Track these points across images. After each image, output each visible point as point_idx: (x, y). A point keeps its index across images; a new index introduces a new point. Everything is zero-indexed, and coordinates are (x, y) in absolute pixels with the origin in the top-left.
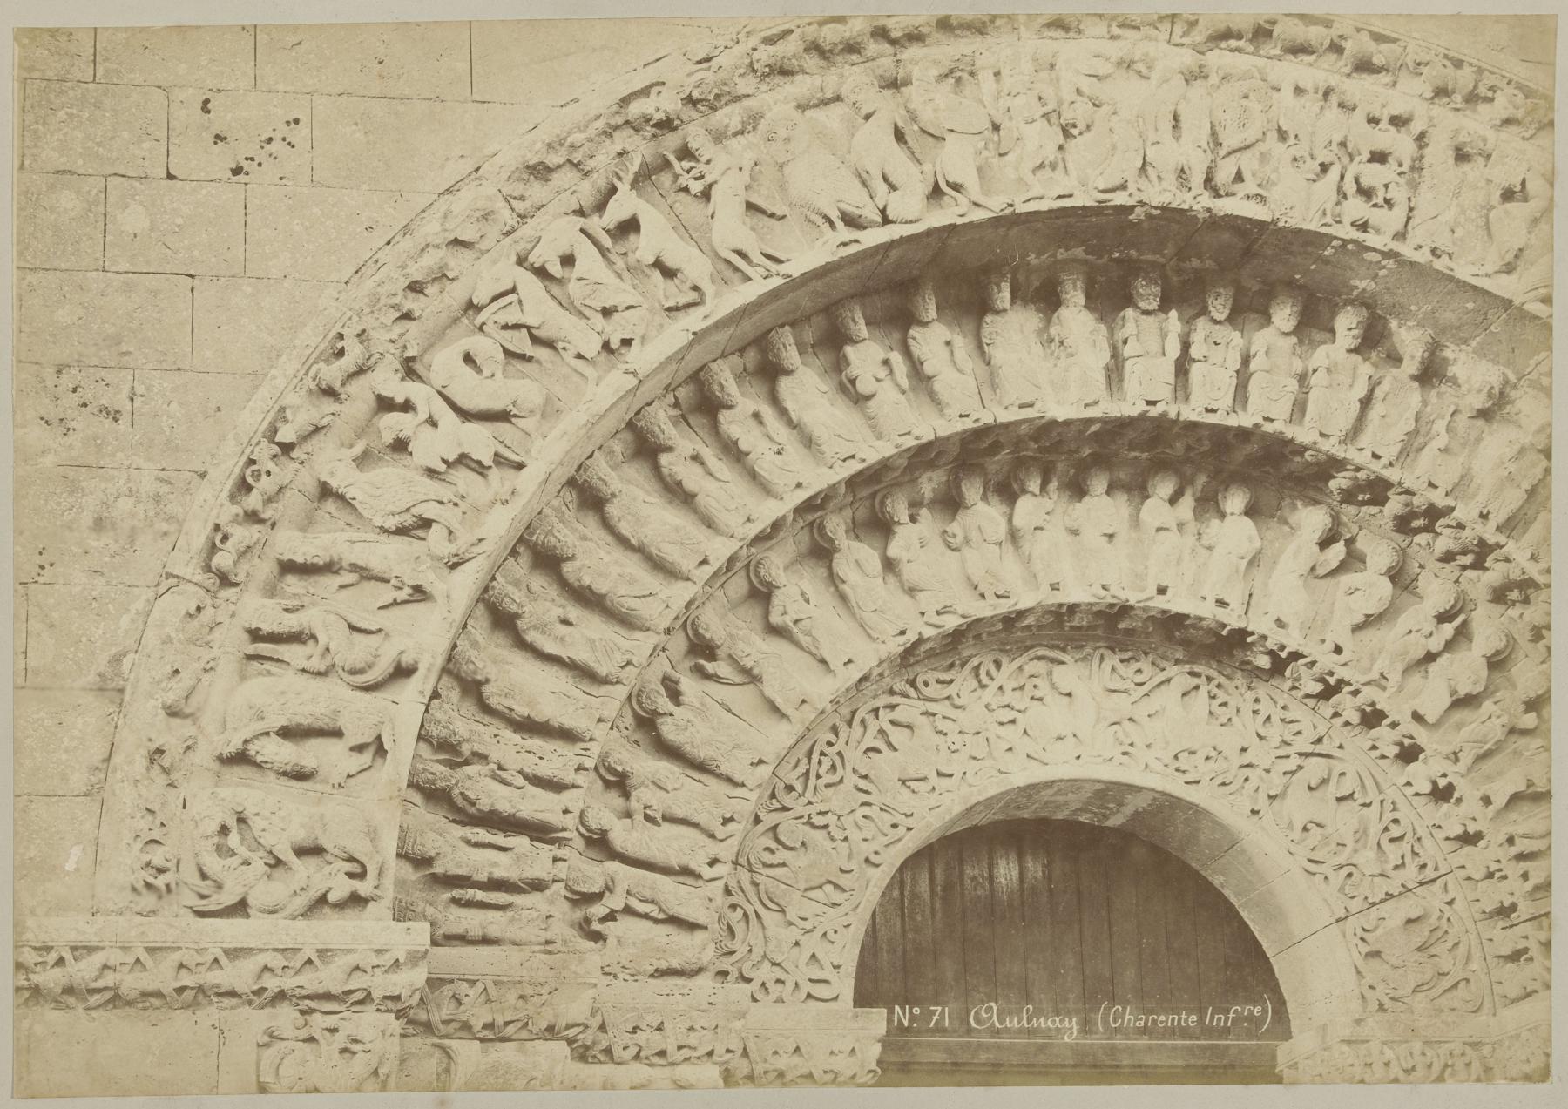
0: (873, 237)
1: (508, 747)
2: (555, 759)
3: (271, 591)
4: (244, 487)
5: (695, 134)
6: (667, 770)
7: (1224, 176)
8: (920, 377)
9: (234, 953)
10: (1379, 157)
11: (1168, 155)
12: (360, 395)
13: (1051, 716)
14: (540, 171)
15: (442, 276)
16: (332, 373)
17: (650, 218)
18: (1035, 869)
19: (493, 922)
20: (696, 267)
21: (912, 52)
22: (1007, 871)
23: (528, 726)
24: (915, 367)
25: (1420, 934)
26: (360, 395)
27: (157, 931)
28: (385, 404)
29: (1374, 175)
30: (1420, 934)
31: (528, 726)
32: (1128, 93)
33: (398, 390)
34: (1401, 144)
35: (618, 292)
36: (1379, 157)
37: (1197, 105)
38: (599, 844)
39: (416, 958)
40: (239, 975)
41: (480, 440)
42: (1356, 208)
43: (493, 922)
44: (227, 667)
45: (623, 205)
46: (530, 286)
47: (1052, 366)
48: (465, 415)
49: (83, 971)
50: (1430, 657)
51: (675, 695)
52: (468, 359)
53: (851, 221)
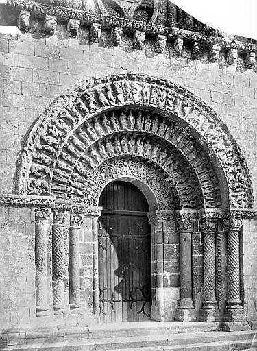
0: (109, 107)
2: (67, 175)
6: (77, 174)
13: (124, 169)
18: (119, 187)
21: (115, 81)
22: (115, 188)
24: (111, 122)
25: (167, 200)
28: (50, 128)
30: (167, 200)
38: (70, 185)
41: (61, 133)
48: (59, 130)
49: (16, 201)
52: (60, 122)
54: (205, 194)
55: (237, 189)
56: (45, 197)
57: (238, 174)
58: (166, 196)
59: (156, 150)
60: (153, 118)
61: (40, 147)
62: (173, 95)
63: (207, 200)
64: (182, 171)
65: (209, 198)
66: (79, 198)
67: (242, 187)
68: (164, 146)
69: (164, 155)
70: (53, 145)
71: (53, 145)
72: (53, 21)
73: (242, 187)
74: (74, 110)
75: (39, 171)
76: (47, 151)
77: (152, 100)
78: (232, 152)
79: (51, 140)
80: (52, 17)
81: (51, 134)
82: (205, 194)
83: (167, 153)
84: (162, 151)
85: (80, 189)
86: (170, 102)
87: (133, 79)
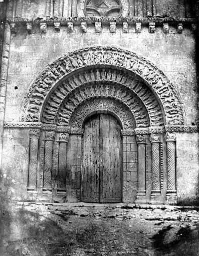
1: (51, 109)
3: (32, 98)
4: (30, 90)
5: (65, 61)
7: (107, 61)
8: (85, 79)
9: (28, 125)
10: (120, 59)
11: (103, 60)
12: (39, 83)
14: (53, 65)
15: (45, 73)
16: (37, 81)
17: (61, 67)
19: (49, 122)
20: (64, 71)
23: (53, 107)
26: (39, 83)
27: (23, 123)
28: (41, 83)
29: (120, 61)
31: (53, 107)
32: (100, 55)
33: (41, 82)
34: (123, 58)
35: (59, 73)
36: (120, 59)
37: (106, 56)
38: (60, 116)
39: (40, 125)
40: (28, 126)
41: (47, 86)
42: (118, 63)
43: (49, 122)
44: (29, 104)
45: (59, 66)
46: (52, 73)
47: (98, 77)
50: (129, 100)
51: (67, 104)
52: (47, 79)
53: (77, 67)
54: (151, 117)
55: (172, 113)
56: (35, 123)
57: (172, 103)
58: (129, 120)
59: (118, 92)
60: (112, 72)
61: (35, 94)
62: (123, 56)
63: (153, 121)
64: (138, 103)
65: (154, 120)
66: (66, 124)
67: (175, 111)
68: (124, 89)
69: (124, 94)
70: (42, 93)
71: (42, 93)
72: (44, 25)
73: (175, 111)
74: (56, 72)
75: (33, 108)
76: (40, 97)
77: (107, 61)
78: (167, 88)
79: (41, 90)
80: (43, 24)
81: (42, 87)
82: (151, 117)
83: (127, 93)
84: (123, 92)
85: (67, 118)
86: (120, 61)
87: (95, 50)
